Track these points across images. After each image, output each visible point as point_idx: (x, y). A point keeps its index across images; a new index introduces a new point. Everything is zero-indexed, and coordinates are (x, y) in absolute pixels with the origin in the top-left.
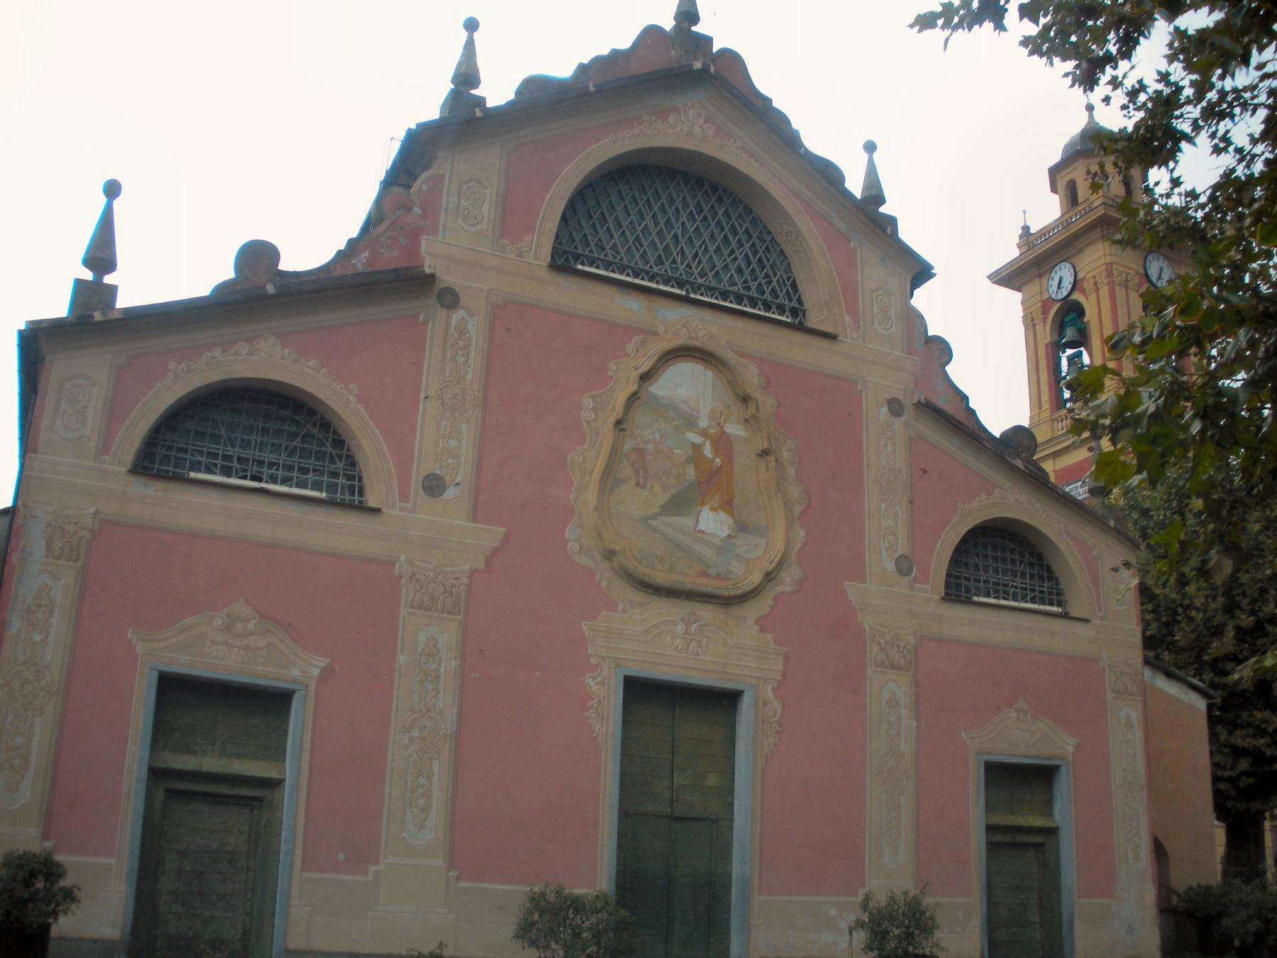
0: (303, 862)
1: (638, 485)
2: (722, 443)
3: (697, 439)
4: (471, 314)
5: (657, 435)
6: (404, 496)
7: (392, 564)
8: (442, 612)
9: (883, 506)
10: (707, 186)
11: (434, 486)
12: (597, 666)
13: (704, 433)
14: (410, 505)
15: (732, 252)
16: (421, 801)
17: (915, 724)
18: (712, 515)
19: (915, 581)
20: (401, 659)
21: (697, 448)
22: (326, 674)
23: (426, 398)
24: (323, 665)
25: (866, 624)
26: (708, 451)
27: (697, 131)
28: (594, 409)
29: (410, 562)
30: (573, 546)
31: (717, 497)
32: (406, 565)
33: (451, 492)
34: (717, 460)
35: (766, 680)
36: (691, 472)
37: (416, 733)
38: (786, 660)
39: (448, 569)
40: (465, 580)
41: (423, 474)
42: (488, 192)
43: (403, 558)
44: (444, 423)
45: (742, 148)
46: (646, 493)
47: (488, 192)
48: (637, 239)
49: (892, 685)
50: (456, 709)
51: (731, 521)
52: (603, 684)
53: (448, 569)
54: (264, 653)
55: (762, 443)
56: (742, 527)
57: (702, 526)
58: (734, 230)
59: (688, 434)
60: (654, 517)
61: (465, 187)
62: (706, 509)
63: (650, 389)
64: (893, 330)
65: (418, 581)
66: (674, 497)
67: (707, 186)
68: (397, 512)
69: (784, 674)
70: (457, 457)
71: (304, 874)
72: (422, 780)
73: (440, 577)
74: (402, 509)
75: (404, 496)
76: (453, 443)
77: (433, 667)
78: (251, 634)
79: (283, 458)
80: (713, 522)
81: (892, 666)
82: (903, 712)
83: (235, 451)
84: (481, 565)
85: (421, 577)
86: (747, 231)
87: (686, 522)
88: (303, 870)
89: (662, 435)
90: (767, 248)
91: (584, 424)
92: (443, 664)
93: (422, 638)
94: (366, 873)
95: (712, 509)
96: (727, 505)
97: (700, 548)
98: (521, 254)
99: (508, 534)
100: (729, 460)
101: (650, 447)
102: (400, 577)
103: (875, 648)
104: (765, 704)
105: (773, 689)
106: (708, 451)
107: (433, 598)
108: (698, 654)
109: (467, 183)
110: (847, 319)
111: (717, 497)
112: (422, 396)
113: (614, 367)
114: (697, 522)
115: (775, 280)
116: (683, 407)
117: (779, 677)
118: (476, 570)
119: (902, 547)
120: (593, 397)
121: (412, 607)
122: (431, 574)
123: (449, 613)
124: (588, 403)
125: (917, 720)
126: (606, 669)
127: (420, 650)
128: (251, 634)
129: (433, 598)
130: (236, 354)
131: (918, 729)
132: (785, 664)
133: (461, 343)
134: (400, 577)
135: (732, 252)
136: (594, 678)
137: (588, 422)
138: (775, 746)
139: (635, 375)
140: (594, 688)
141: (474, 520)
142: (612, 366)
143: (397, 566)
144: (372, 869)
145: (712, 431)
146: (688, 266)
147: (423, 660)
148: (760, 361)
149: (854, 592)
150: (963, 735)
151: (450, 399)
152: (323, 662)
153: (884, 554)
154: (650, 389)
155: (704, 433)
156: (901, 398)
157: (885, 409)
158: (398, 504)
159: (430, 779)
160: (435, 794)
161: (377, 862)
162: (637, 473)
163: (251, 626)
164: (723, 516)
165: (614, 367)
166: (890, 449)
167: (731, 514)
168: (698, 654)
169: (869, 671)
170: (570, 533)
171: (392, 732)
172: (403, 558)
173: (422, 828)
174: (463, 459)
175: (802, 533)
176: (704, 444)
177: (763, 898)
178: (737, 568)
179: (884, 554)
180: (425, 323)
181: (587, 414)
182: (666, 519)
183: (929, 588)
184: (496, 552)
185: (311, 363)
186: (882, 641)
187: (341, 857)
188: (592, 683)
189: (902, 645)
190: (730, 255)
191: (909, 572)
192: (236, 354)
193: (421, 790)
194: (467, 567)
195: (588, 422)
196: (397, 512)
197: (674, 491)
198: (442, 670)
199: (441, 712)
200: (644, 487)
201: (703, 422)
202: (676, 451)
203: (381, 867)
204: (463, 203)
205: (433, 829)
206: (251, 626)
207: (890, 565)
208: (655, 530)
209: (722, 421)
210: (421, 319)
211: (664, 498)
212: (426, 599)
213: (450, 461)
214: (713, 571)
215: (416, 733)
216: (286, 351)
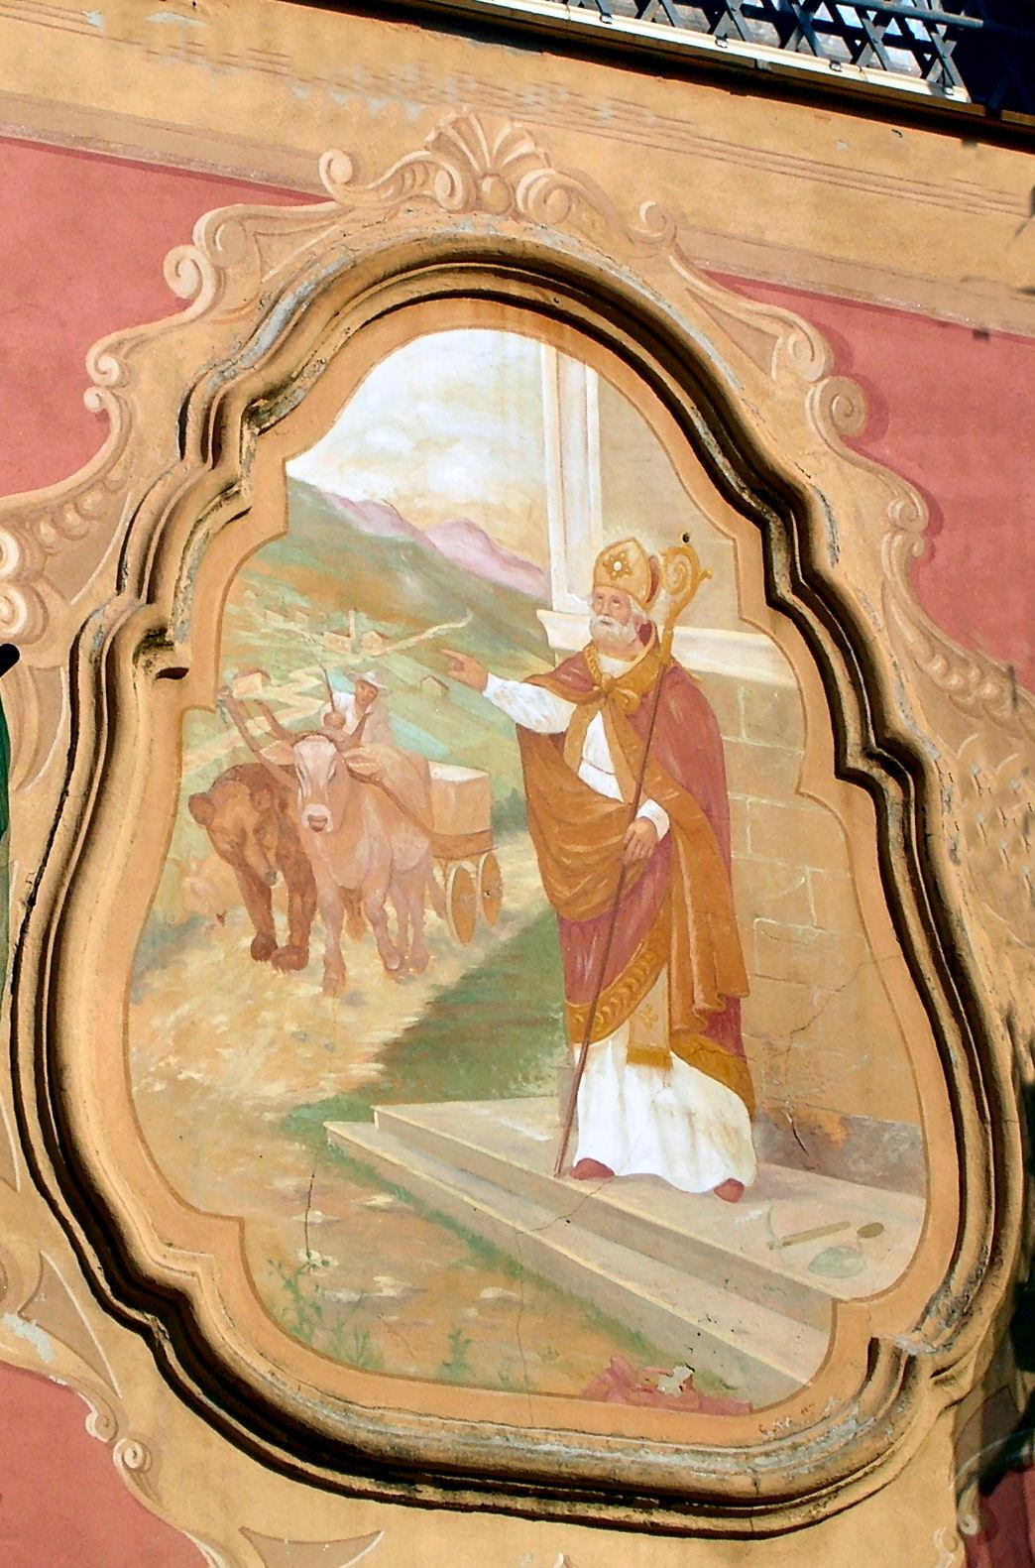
1: (264, 949)
2: (668, 718)
3: (548, 712)
5: (345, 698)
13: (574, 678)
18: (640, 1084)
21: (545, 751)
26: (599, 766)
34: (649, 809)
36: (521, 874)
46: (306, 988)
57: (590, 1145)
60: (358, 1103)
62: (608, 1053)
63: (296, 469)
66: (443, 1005)
87: (516, 1123)
89: (367, 696)
95: (639, 1056)
96: (715, 1033)
97: (587, 1255)
101: (315, 756)
106: (599, 766)
116: (467, 552)
142: (102, 363)
145: (613, 666)
148: (835, 312)
154: (296, 469)
155: (574, 678)
162: (258, 892)
164: (694, 1087)
165: (110, 364)
176: (579, 726)
182: (408, 1114)
197: (447, 974)
200: (295, 958)
201: (569, 625)
202: (442, 773)
208: (370, 1174)
209: (658, 614)
211: (393, 1011)
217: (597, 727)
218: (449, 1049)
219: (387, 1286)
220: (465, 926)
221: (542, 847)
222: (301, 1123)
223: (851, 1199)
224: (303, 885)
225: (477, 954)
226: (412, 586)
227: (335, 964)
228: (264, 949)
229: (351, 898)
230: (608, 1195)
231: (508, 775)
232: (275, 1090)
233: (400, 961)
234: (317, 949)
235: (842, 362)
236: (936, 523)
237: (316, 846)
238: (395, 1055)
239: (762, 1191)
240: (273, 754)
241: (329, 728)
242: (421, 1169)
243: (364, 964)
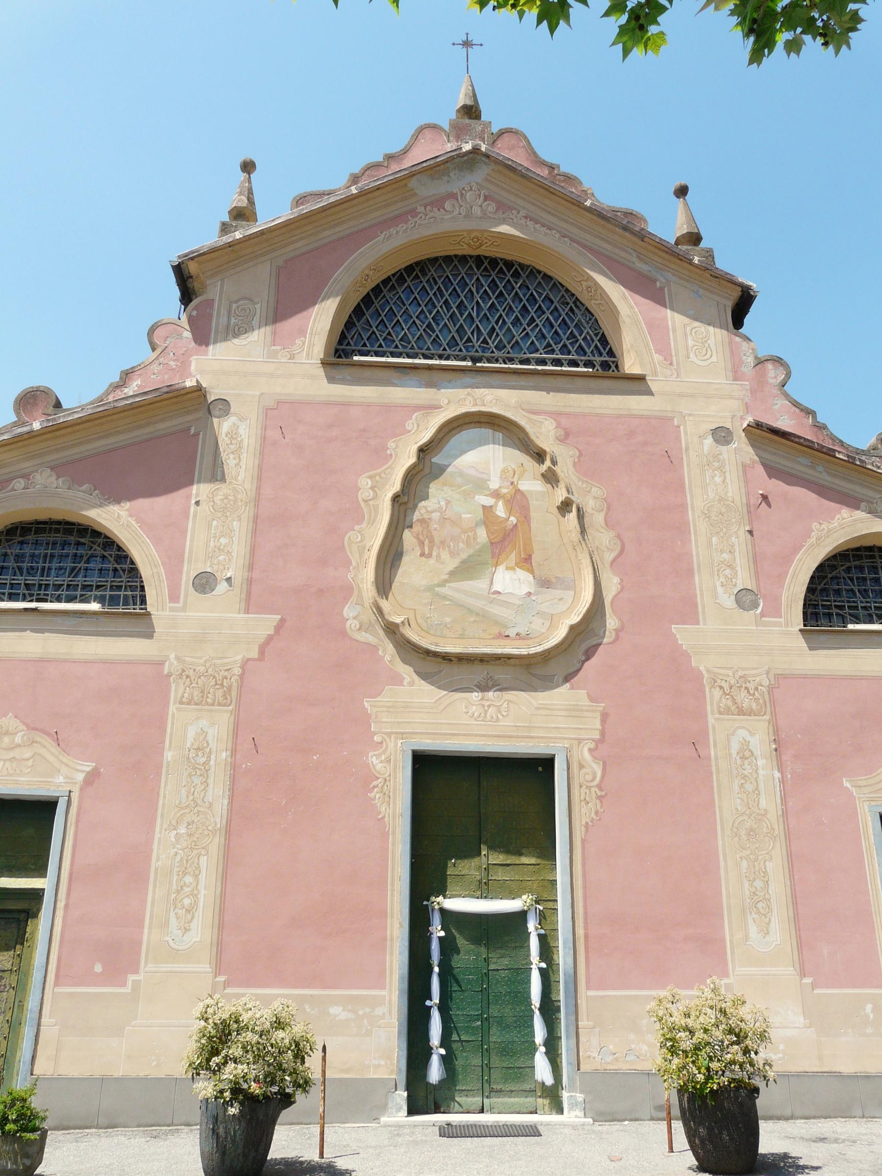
0: (57, 976)
1: (422, 555)
2: (518, 501)
3: (489, 501)
4: (242, 419)
5: (443, 503)
6: (174, 597)
7: (161, 664)
8: (213, 705)
9: (714, 539)
10: (501, 265)
11: (204, 583)
12: (382, 742)
13: (496, 495)
14: (180, 605)
15: (532, 320)
16: (187, 902)
17: (777, 775)
18: (508, 575)
19: (762, 615)
20: (169, 755)
21: (487, 510)
22: (91, 778)
23: (197, 503)
24: (88, 769)
25: (702, 668)
26: (501, 511)
27: (477, 211)
28: (372, 488)
29: (178, 658)
30: (352, 625)
31: (513, 556)
32: (175, 663)
33: (222, 587)
34: (512, 518)
35: (580, 741)
36: (482, 535)
37: (182, 830)
38: (604, 717)
39: (218, 662)
40: (237, 671)
41: (193, 575)
42: (258, 306)
43: (172, 656)
44: (215, 523)
45: (526, 217)
46: (432, 561)
47: (258, 306)
48: (429, 326)
49: (742, 733)
50: (226, 802)
51: (531, 578)
52: (388, 761)
53: (218, 662)
54: (30, 763)
55: (561, 494)
56: (545, 583)
57: (497, 587)
58: (532, 299)
59: (477, 497)
60: (443, 584)
61: (234, 306)
62: (501, 569)
63: (433, 460)
64: (714, 359)
65: (188, 677)
66: (463, 562)
67: (501, 265)
68: (168, 613)
69: (603, 733)
70: (229, 553)
71: (57, 990)
72: (188, 879)
73: (210, 671)
74: (172, 609)
75: (174, 597)
76: (223, 541)
77: (203, 760)
78: (19, 746)
79: (64, 580)
80: (510, 581)
81: (741, 712)
82: (761, 762)
83: (20, 579)
84: (255, 654)
85: (191, 673)
86: (547, 297)
87: (479, 585)
88: (56, 984)
89: (448, 502)
90: (571, 309)
91: (362, 504)
92: (213, 757)
93: (191, 733)
94: (124, 984)
95: (507, 568)
96: (526, 562)
97: (495, 610)
98: (292, 357)
99: (282, 621)
100: (526, 517)
101: (436, 516)
102: (169, 675)
103: (717, 693)
104: (581, 767)
105: (590, 750)
106: (501, 511)
107: (203, 692)
108: (498, 720)
109: (236, 302)
110: (657, 357)
111: (513, 556)
112: (193, 502)
113: (394, 445)
114: (492, 583)
115: (580, 338)
116: (472, 472)
117: (597, 736)
118: (249, 660)
119: (744, 579)
120: (370, 477)
121: (181, 703)
122: (202, 669)
123: (220, 704)
124: (365, 482)
125: (781, 770)
126: (391, 745)
127: (188, 745)
128: (19, 746)
129: (203, 692)
130: (13, 490)
131: (783, 781)
132: (603, 722)
133: (232, 447)
134: (169, 675)
135: (532, 320)
136: (378, 756)
137: (365, 501)
138: (597, 813)
139: (414, 448)
140: (379, 767)
141: (247, 611)
142: (391, 444)
143: (167, 664)
144: (131, 978)
145: (504, 491)
146: (485, 341)
147: (192, 754)
148: (556, 415)
149: (684, 635)
150: (847, 784)
151: (222, 500)
152: (88, 767)
153: (720, 590)
154: (433, 460)
155: (496, 495)
156: (729, 426)
157: (709, 441)
158: (169, 605)
159: (196, 876)
160: (203, 892)
161: (136, 971)
162: (422, 543)
163: (18, 739)
164: (522, 575)
165: (394, 445)
166: (718, 479)
167: (531, 571)
168: (498, 720)
169: (711, 720)
170: (349, 611)
171: (158, 829)
172: (172, 656)
173: (186, 930)
174: (234, 554)
175: (616, 580)
176: (496, 504)
177: (591, 993)
178: (538, 625)
179: (720, 590)
180: (197, 435)
181: (365, 493)
182: (452, 585)
183: (782, 620)
184: (270, 638)
185: (84, 487)
186: (726, 686)
187: (98, 968)
188: (375, 761)
189: (751, 686)
190: (529, 325)
191: (755, 605)
192: (13, 490)
193: (186, 889)
194: (239, 657)
195: (365, 501)
196: (168, 613)
197: (464, 556)
198: (212, 762)
199: (211, 804)
200: (430, 556)
201: (494, 484)
202: (463, 516)
203: (140, 977)
204: (233, 320)
205: (199, 932)
206: (18, 739)
207: (729, 602)
208: (445, 598)
210: (192, 431)
211: (452, 564)
212: (196, 693)
213: (221, 558)
214: (512, 633)
215: (182, 830)
216: (60, 480)
217: (500, 503)
218: (467, 569)
219: (448, 620)
220: (468, 544)
221: (487, 527)
222: (430, 589)
223: (557, 593)
224: (432, 541)
225: (471, 551)
226: (459, 480)
227: (438, 556)
228: (422, 555)
229: (443, 543)
230: (500, 597)
231: (480, 514)
232: (424, 582)
233: (452, 554)
234: (434, 554)
235: (559, 426)
236: (581, 455)
237: (435, 533)
238: (452, 574)
239: (537, 593)
240: (426, 516)
241: (439, 510)
242: (456, 595)
243: (445, 555)
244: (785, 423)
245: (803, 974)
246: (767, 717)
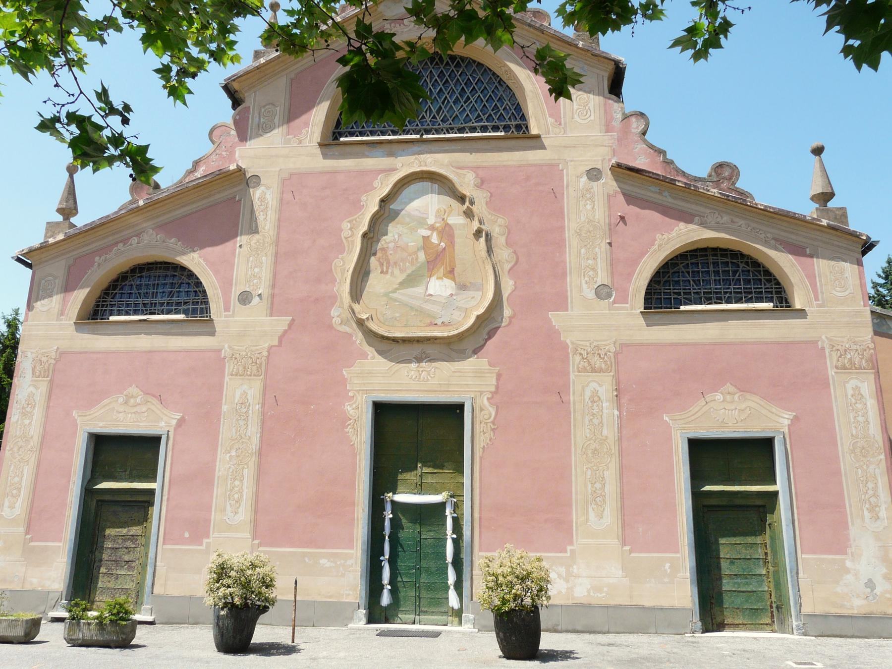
1: (382, 272)
2: (447, 232)
3: (426, 233)
4: (268, 188)
5: (396, 236)
6: (227, 309)
7: (220, 351)
9: (583, 251)
11: (245, 298)
13: (432, 228)
14: (231, 313)
15: (468, 98)
16: (236, 496)
17: (616, 413)
18: (438, 282)
19: (614, 302)
20: (225, 408)
21: (426, 239)
22: (181, 423)
23: (240, 246)
25: (568, 341)
26: (435, 239)
28: (351, 229)
29: (230, 347)
30: (336, 321)
31: (442, 270)
33: (256, 300)
35: (481, 393)
36: (422, 256)
37: (234, 454)
38: (499, 376)
40: (265, 354)
43: (226, 346)
44: (251, 259)
46: (388, 276)
49: (594, 385)
54: (146, 414)
55: (476, 225)
56: (462, 287)
57: (430, 291)
60: (394, 291)
61: (263, 110)
62: (433, 279)
64: (592, 118)
69: (497, 387)
71: (165, 547)
72: (237, 483)
74: (226, 316)
75: (227, 309)
76: (256, 270)
79: (165, 300)
80: (439, 287)
81: (594, 370)
82: (604, 405)
84: (276, 343)
87: (418, 290)
88: (164, 543)
89: (400, 235)
91: (344, 240)
93: (238, 394)
94: (201, 544)
96: (451, 273)
97: (428, 307)
98: (300, 142)
99: (293, 320)
101: (391, 245)
103: (578, 358)
104: (482, 410)
105: (488, 399)
106: (435, 239)
109: (264, 106)
110: (550, 120)
111: (442, 270)
116: (417, 213)
117: (493, 389)
119: (602, 277)
120: (349, 222)
121: (232, 375)
122: (244, 353)
124: (346, 225)
125: (619, 409)
126: (359, 398)
130: (131, 245)
131: (620, 417)
132: (498, 379)
135: (468, 98)
136: (351, 405)
137: (346, 238)
140: (351, 412)
141: (271, 315)
142: (364, 198)
144: (205, 541)
145: (438, 225)
146: (434, 117)
148: (475, 169)
149: (556, 318)
150: (666, 418)
152: (178, 416)
153: (584, 286)
155: (432, 228)
156: (599, 167)
157: (584, 179)
159: (242, 481)
160: (245, 490)
162: (381, 265)
163: (138, 400)
164: (448, 282)
166: (589, 207)
167: (454, 280)
169: (572, 376)
170: (334, 312)
172: (226, 346)
175: (511, 282)
176: (432, 234)
177: (482, 554)
178: (457, 316)
179: (584, 286)
180: (240, 201)
181: (346, 233)
183: (628, 305)
184: (285, 332)
186: (584, 353)
187: (187, 535)
188: (349, 409)
189: (602, 353)
190: (465, 103)
191: (609, 296)
192: (131, 245)
193: (236, 489)
194: (266, 345)
195: (346, 238)
197: (409, 272)
201: (431, 221)
203: (210, 540)
204: (262, 120)
205: (244, 514)
207: (591, 294)
208: (396, 300)
209: (445, 217)
210: (237, 199)
211: (401, 277)
213: (255, 281)
214: (439, 322)
217: (435, 234)
218: (411, 280)
219: (397, 315)
220: (412, 264)
221: (425, 251)
222: (386, 295)
223: (471, 293)
224: (388, 263)
225: (414, 268)
226: (408, 220)
227: (392, 273)
228: (382, 272)
229: (395, 263)
230: (432, 298)
231: (420, 242)
232: (382, 291)
233: (402, 271)
234: (390, 271)
235: (477, 176)
236: (491, 196)
237: (390, 257)
238: (401, 284)
239: (457, 294)
240: (385, 246)
241: (394, 241)
243: (397, 272)
244: (641, 162)
245: (624, 543)
246: (612, 374)
